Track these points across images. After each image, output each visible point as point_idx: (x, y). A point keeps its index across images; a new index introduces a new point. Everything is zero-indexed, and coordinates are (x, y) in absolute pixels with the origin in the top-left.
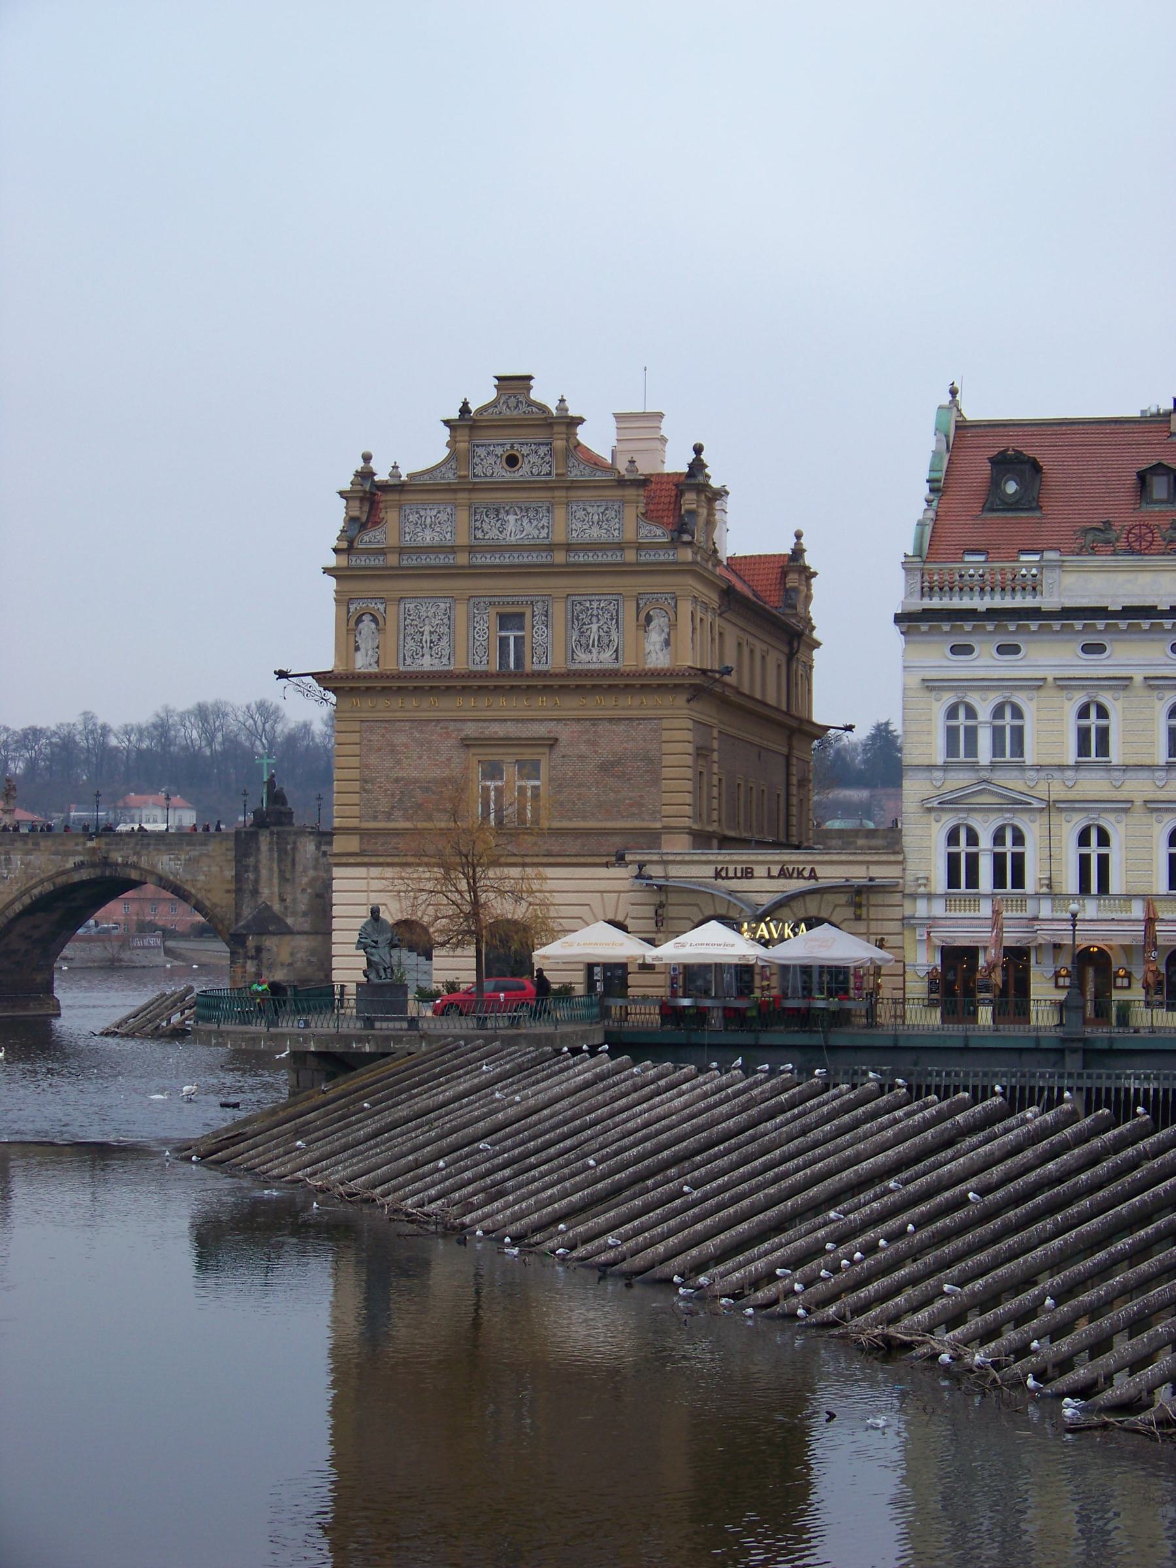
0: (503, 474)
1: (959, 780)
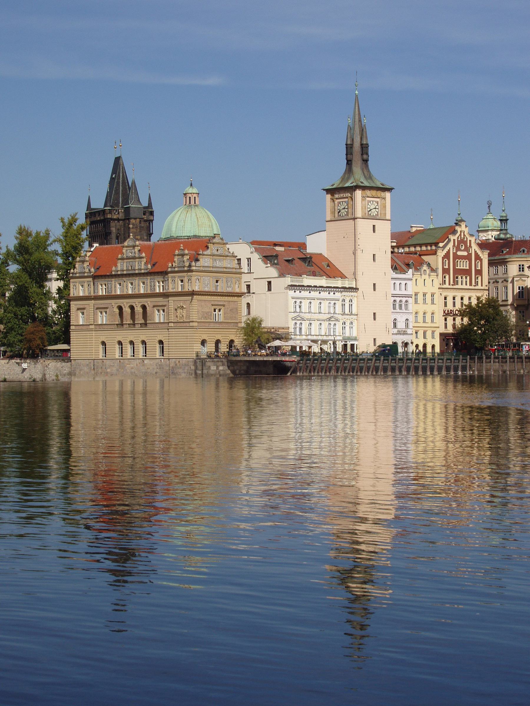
0: (216, 253)
1: (296, 314)
